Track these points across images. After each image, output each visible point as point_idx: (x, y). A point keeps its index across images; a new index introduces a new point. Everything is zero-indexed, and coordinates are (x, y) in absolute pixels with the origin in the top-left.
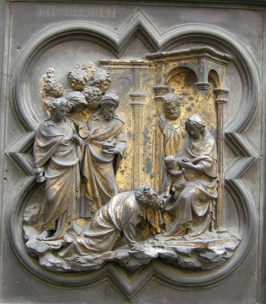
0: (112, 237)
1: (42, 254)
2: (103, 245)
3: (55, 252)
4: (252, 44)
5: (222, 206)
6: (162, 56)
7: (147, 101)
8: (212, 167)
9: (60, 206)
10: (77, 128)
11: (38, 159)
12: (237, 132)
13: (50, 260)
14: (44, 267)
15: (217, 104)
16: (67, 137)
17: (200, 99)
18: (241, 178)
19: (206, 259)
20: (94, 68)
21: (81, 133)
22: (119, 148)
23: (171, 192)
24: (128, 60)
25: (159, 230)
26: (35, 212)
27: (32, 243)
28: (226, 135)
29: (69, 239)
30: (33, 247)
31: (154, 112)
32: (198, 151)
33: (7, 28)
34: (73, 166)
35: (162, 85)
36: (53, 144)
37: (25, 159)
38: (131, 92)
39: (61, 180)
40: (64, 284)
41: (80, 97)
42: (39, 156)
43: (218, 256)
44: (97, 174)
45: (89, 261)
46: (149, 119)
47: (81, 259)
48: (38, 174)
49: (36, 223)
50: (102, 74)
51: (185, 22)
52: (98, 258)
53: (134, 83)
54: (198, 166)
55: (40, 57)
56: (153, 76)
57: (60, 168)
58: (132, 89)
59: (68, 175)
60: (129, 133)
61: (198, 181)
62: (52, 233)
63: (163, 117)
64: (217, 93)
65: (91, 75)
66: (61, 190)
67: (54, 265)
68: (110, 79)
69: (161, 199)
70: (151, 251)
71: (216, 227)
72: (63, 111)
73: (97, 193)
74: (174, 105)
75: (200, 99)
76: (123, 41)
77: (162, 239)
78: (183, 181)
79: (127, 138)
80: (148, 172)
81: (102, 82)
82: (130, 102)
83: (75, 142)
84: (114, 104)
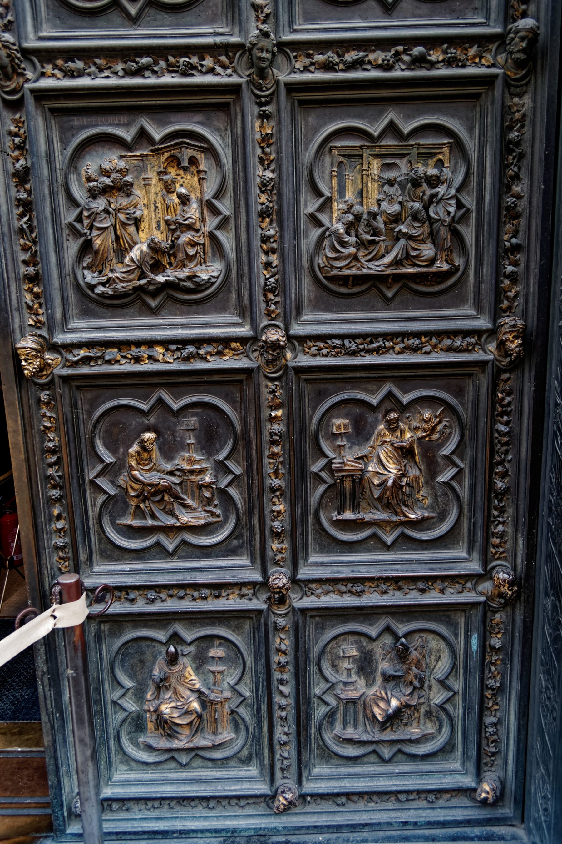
0: (136, 271)
1: (95, 286)
2: (131, 277)
3: (103, 284)
4: (221, 136)
5: (208, 248)
6: (159, 149)
7: (154, 181)
8: (195, 222)
9: (102, 254)
10: (110, 203)
11: (85, 225)
12: (216, 199)
13: (100, 289)
14: (98, 295)
15: (200, 180)
16: (101, 208)
17: (188, 177)
18: (218, 229)
19: (196, 282)
20: (116, 161)
21: (112, 206)
22: (138, 214)
23: (172, 241)
24: (138, 153)
25: (168, 267)
26: (90, 260)
27: (88, 279)
28: (207, 201)
29: (111, 275)
30: (89, 281)
31: (159, 189)
32: (187, 212)
33: (54, 135)
34: (107, 228)
35: (162, 170)
36: (93, 213)
37: (78, 226)
38: (143, 176)
39: (101, 237)
40: (112, 306)
41: (108, 181)
42: (86, 222)
43: (203, 280)
44: (125, 233)
45: (123, 287)
46: (156, 194)
47: (119, 287)
48: (86, 234)
49: (91, 267)
50: (122, 164)
51: (174, 123)
52: (130, 286)
53: (143, 169)
54: (186, 222)
55: (80, 155)
56: (156, 164)
57: (99, 229)
58: (143, 174)
59: (105, 234)
60: (144, 204)
61: (188, 232)
62: (100, 272)
63: (164, 191)
64: (199, 172)
65: (114, 166)
66: (101, 244)
67: (103, 292)
68: (127, 167)
69: (164, 245)
70: (161, 279)
71: (205, 262)
72: (95, 190)
73: (127, 245)
74: (170, 182)
75: (188, 177)
76: (133, 140)
77: (169, 272)
78: (178, 233)
79: (143, 208)
80: (159, 229)
81: (121, 170)
82: (143, 183)
83: (106, 211)
84: (131, 185)
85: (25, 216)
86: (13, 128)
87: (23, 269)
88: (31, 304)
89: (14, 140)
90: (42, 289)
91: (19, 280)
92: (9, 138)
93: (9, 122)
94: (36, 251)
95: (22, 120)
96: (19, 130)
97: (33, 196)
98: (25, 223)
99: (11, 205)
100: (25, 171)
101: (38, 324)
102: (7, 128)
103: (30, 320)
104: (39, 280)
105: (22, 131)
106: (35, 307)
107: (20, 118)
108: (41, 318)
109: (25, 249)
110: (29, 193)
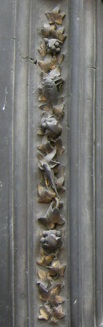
85: (50, 151)
86: (47, 26)
87: (39, 231)
88: (44, 285)
89: (46, 43)
90: (65, 264)
91: (32, 249)
92: (40, 39)
93: (43, 17)
94: (61, 206)
95: (62, 14)
96: (56, 29)
97: (65, 122)
98: (51, 163)
99: (32, 136)
100: (58, 86)
101: (53, 319)
102: (39, 26)
103: (42, 312)
104: (60, 250)
105: (60, 30)
106: (52, 292)
107: (59, 12)
108: (60, 309)
109: (45, 201)
110: (60, 117)
